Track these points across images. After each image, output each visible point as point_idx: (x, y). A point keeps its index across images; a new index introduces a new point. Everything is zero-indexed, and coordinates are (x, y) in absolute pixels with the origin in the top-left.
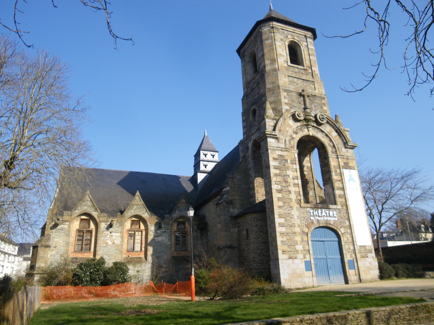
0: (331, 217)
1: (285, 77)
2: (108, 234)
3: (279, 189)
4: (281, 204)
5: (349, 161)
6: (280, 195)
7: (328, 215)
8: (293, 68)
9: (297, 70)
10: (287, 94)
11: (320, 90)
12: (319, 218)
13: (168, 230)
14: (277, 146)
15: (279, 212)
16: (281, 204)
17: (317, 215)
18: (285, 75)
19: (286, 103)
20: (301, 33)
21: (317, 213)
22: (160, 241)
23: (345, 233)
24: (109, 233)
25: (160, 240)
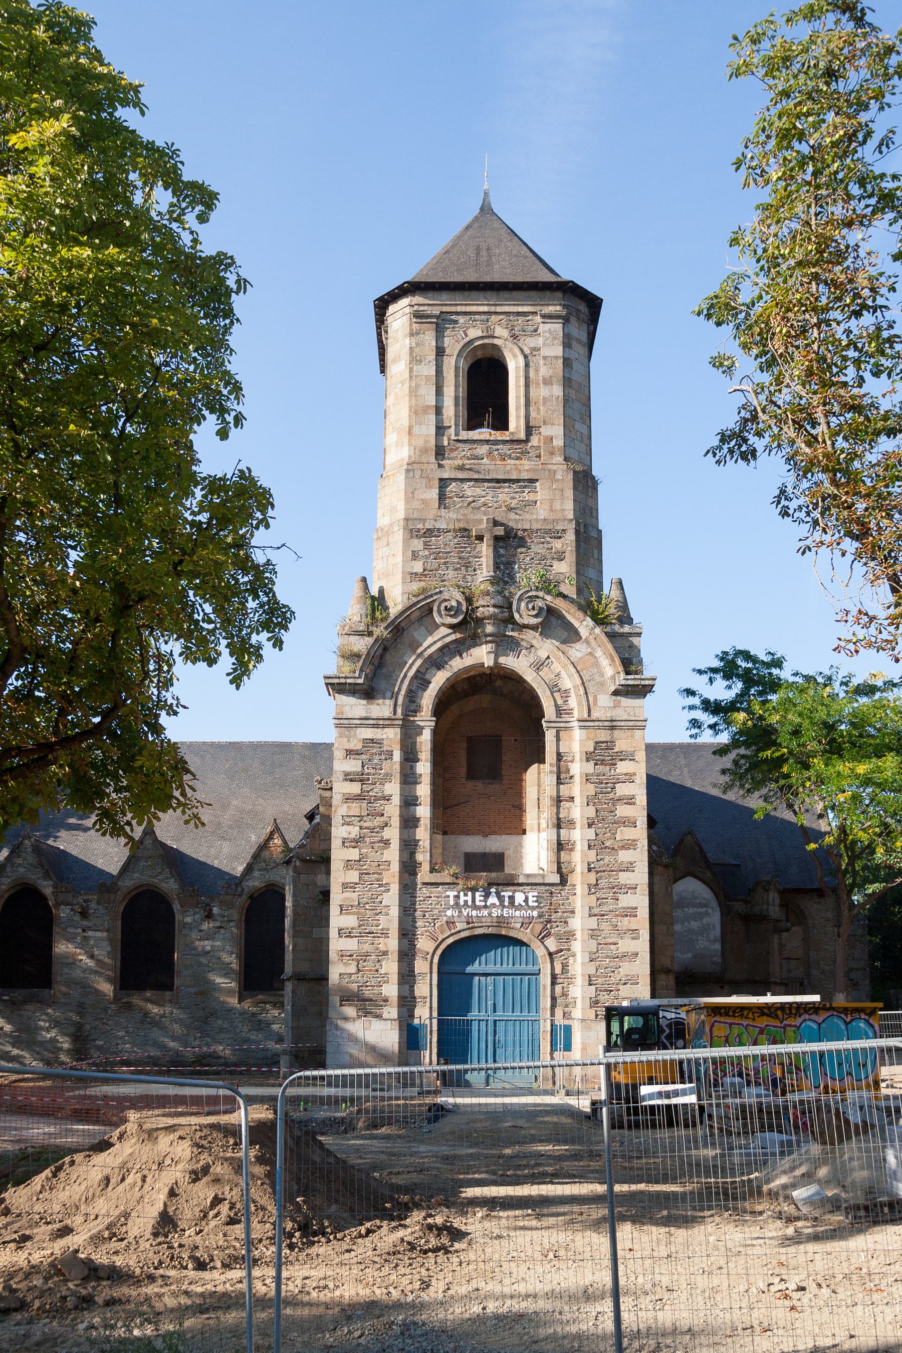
1: (429, 487)
2: (77, 934)
3: (352, 836)
4: (353, 876)
5: (616, 732)
6: (354, 854)
7: (506, 904)
10: (425, 544)
11: (557, 506)
12: (474, 913)
14: (364, 714)
15: (346, 899)
16: (353, 876)
17: (470, 903)
18: (430, 480)
19: (416, 574)
21: (469, 898)
22: (209, 952)
23: (561, 951)
24: (80, 930)
25: (208, 948)
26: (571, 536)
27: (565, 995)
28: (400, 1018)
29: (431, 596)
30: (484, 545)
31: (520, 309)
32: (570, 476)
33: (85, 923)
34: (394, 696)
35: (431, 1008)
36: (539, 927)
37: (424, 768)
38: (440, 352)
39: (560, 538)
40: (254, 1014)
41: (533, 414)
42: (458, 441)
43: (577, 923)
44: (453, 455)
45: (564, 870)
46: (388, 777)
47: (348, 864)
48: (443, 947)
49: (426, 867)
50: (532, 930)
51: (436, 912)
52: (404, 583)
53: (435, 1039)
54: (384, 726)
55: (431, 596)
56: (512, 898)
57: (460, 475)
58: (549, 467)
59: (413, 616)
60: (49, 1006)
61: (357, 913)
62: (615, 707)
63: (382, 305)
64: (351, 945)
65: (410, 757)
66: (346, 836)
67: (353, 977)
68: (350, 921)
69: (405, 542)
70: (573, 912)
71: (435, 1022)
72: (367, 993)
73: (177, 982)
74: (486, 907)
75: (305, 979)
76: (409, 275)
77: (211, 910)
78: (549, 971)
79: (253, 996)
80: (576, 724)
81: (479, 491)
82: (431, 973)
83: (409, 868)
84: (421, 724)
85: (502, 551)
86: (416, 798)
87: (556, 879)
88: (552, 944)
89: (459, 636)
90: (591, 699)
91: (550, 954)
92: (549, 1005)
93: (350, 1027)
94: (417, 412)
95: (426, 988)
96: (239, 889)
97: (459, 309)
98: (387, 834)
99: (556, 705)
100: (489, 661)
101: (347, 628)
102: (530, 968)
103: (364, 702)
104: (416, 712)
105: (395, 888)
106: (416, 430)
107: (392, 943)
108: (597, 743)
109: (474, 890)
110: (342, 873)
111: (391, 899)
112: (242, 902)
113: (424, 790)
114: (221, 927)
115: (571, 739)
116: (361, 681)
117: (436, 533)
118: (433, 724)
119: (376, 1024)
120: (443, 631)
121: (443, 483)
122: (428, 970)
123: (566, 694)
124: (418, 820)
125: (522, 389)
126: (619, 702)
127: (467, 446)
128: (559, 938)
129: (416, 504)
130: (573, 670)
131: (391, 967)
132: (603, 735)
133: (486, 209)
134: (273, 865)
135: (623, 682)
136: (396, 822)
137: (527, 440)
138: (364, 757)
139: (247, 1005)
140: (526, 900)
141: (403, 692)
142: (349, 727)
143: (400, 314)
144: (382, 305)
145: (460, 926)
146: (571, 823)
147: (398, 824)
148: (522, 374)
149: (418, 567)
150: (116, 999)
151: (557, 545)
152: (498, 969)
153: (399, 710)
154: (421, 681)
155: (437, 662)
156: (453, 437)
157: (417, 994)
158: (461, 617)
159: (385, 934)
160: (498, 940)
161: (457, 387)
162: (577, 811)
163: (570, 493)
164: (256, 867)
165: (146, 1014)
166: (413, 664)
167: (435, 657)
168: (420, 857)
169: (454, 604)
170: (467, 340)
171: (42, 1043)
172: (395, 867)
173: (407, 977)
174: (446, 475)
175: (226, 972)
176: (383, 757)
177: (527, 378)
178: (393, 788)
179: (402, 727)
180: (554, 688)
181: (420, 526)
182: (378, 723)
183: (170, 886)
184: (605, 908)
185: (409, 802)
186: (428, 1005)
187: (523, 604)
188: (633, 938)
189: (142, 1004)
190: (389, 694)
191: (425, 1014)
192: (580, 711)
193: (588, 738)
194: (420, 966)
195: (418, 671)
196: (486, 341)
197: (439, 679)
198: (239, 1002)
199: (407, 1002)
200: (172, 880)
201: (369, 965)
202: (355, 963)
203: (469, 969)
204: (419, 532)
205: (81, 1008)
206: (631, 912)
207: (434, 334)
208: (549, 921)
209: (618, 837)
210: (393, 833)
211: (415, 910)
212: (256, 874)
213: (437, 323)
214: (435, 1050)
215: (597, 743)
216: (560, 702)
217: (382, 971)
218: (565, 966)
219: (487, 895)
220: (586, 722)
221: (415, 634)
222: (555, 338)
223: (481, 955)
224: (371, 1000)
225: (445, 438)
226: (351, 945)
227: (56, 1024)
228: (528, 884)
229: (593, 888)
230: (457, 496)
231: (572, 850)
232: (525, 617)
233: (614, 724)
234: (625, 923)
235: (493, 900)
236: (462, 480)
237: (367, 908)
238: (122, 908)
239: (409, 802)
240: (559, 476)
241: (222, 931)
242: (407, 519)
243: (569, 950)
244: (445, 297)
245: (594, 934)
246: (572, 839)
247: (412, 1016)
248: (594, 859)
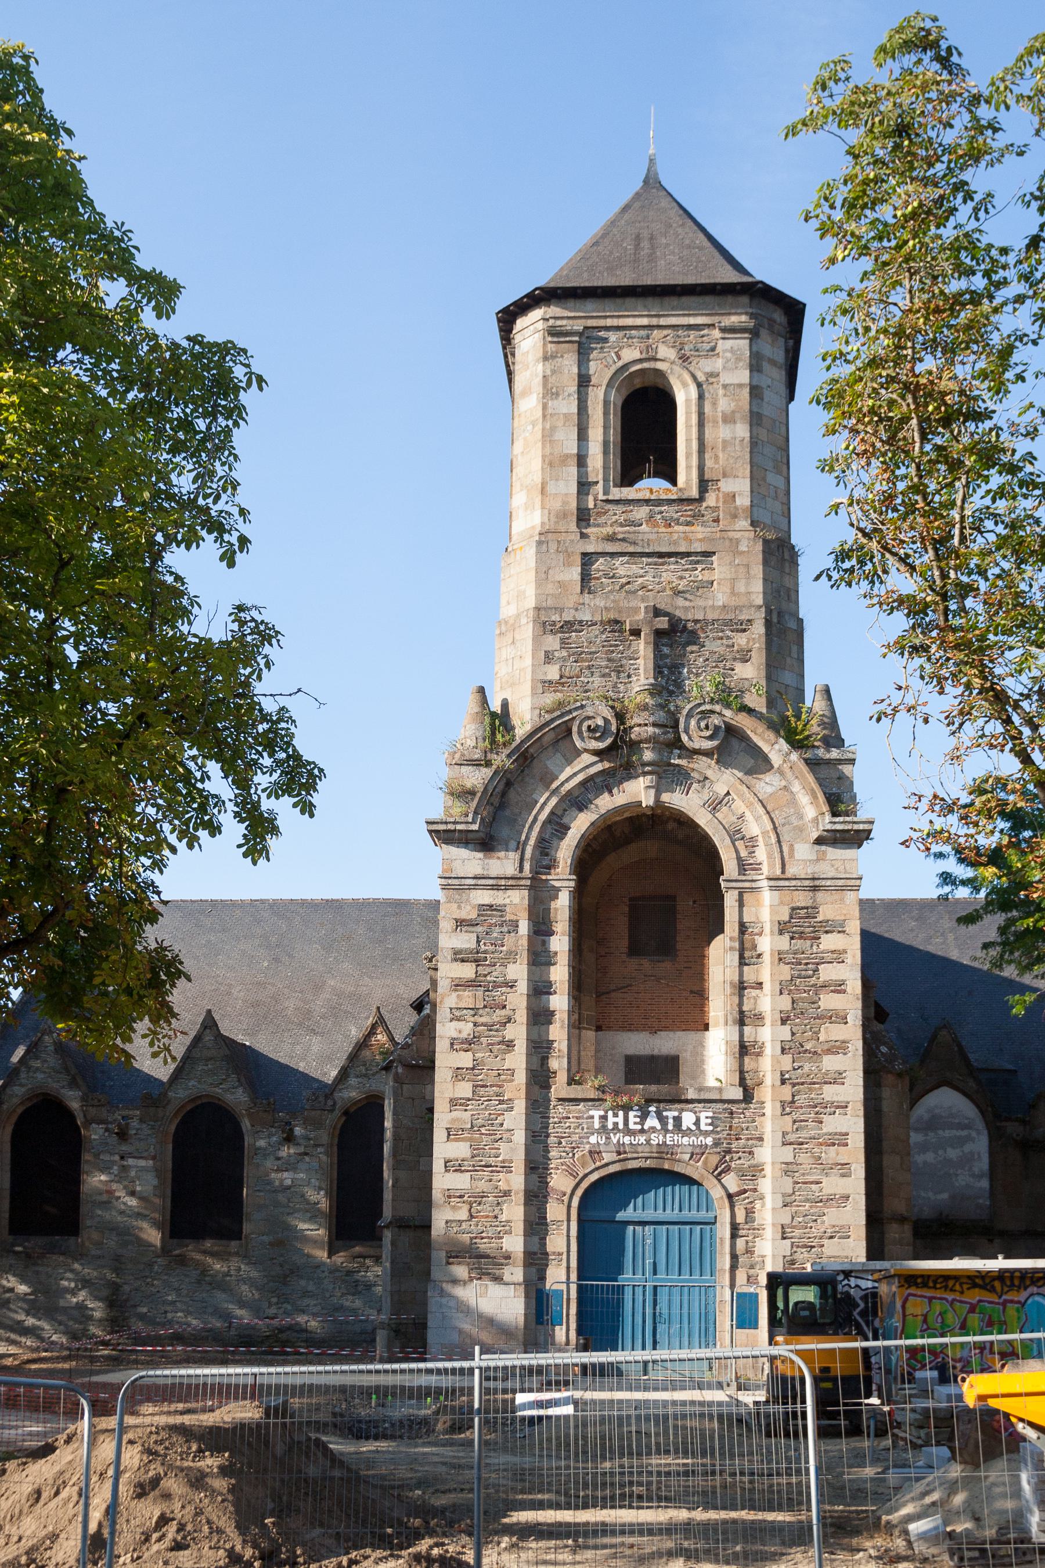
0: (688, 1132)
1: (568, 564)
2: (114, 1162)
3: (464, 1035)
4: (464, 1089)
5: (820, 895)
6: (465, 1060)
7: (670, 1127)
10: (564, 642)
11: (741, 587)
12: (627, 1140)
13: (317, 1146)
14: (479, 871)
15: (454, 1120)
16: (464, 1089)
17: (621, 1126)
18: (569, 555)
21: (620, 1120)
22: (289, 1188)
23: (745, 1191)
24: (117, 1158)
25: (289, 1182)
26: (759, 629)
27: (749, 1251)
28: (527, 1283)
29: (570, 712)
30: (642, 641)
31: (692, 321)
32: (759, 547)
33: (124, 1148)
34: (521, 847)
35: (568, 1268)
36: (714, 1160)
37: (560, 943)
38: (584, 381)
39: (744, 631)
40: (349, 1273)
41: (709, 463)
42: (607, 501)
43: (767, 1154)
44: (602, 520)
45: (749, 1082)
46: (511, 956)
47: (458, 1074)
48: (585, 1185)
49: (562, 1077)
50: (705, 1163)
51: (575, 1137)
52: (534, 694)
53: (573, 1310)
54: (507, 888)
55: (570, 712)
56: (678, 1120)
57: (610, 548)
58: (731, 534)
59: (546, 739)
60: (76, 1259)
61: (470, 1140)
62: (818, 860)
63: (508, 318)
64: (461, 1182)
65: (541, 928)
66: (455, 1035)
67: (464, 1226)
68: (460, 1150)
69: (536, 640)
70: (761, 1139)
71: (574, 1288)
72: (484, 1246)
73: (247, 1228)
74: (642, 1131)
75: (409, 1227)
76: (543, 278)
77: (291, 1130)
78: (728, 1219)
79: (346, 1248)
80: (765, 883)
81: (635, 569)
82: (569, 1220)
83: (539, 1078)
84: (557, 884)
85: (666, 650)
86: (550, 984)
87: (737, 1093)
88: (731, 1182)
89: (607, 765)
90: (785, 849)
91: (730, 1196)
92: (727, 1266)
93: (460, 1292)
94: (552, 463)
95: (562, 1240)
96: (330, 1103)
97: (609, 322)
98: (510, 1032)
99: (739, 858)
100: (647, 800)
101: (457, 756)
102: (703, 1215)
103: (480, 855)
104: (549, 868)
105: (520, 1106)
106: (551, 488)
107: (516, 1180)
108: (793, 909)
109: (627, 1108)
110: (450, 1085)
111: (516, 1120)
112: (333, 1119)
113: (560, 974)
114: (306, 1154)
115: (759, 904)
116: (475, 827)
117: (577, 627)
118: (572, 884)
119: (495, 1290)
120: (587, 759)
121: (587, 559)
122: (564, 1217)
124: (552, 1013)
125: (694, 430)
126: (824, 853)
127: (620, 508)
128: (742, 1174)
129: (550, 589)
130: (761, 810)
131: (515, 1212)
132: (802, 899)
133: (652, 183)
134: (375, 1069)
135: (829, 827)
136: (522, 1017)
137: (701, 499)
138: (479, 929)
139: (339, 1259)
140: (697, 1123)
141: (532, 842)
142: (460, 889)
143: (531, 328)
144: (508, 318)
145: (607, 1157)
146: (759, 1018)
147: (524, 1020)
148: (694, 408)
149: (553, 673)
150: (165, 1250)
152: (660, 1215)
153: (527, 866)
154: (557, 826)
156: (601, 497)
157: (549, 1248)
158: (609, 741)
159: (506, 1167)
160: (659, 1176)
161: (606, 428)
162: (767, 1002)
163: (758, 570)
164: (352, 1072)
165: (204, 1271)
166: (546, 804)
168: (554, 1064)
169: (600, 722)
170: (620, 364)
171: (65, 1310)
172: (521, 1077)
173: (536, 1226)
174: (591, 548)
175: (312, 1213)
176: (505, 929)
177: (701, 414)
178: (519, 971)
179: (531, 888)
180: (735, 835)
181: (555, 617)
182: (499, 884)
183: (237, 1097)
184: (804, 1134)
185: (540, 989)
186: (564, 1263)
187: (693, 722)
188: (843, 1176)
189: (198, 1257)
190: (513, 844)
191: (560, 1277)
192: (771, 866)
193: (782, 903)
194: (554, 1211)
195: (552, 813)
196: (646, 365)
197: (581, 824)
198: (329, 1257)
199: (536, 1260)
200: (240, 1090)
201: (485, 1210)
202: (466, 1207)
203: (621, 1216)
204: (555, 625)
205: (117, 1263)
206: (840, 1140)
207: (575, 357)
208: (729, 1151)
209: (822, 1037)
210: (518, 1032)
211: (548, 1136)
212: (353, 1081)
213: (579, 343)
214: (573, 1326)
215: (793, 909)
216: (743, 854)
217: (503, 1217)
218: (749, 1212)
219: (644, 1117)
220: (780, 881)
221: (550, 764)
222: (738, 359)
223: (636, 1197)
224: (488, 1257)
225: (591, 498)
226: (461, 1182)
227: (85, 1283)
228: (699, 1101)
229: (787, 1106)
230: (606, 576)
231: (759, 1054)
232: (696, 739)
233: (817, 883)
234: (832, 1154)
235: (652, 1122)
236: (613, 555)
237: (483, 1133)
238: (173, 1127)
239: (540, 989)
240: (743, 547)
241: (307, 1159)
242: (538, 609)
243: (755, 1190)
244: (590, 307)
245: (788, 1169)
246: (760, 1039)
247: (542, 1278)
248: (789, 1067)
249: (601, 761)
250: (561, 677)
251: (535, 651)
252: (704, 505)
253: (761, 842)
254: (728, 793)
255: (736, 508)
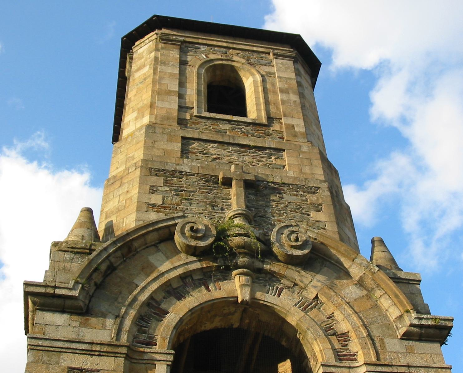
8: (210, 122)
9: (227, 127)
14: (72, 336)
19: (154, 205)
20: (255, 49)
29: (173, 219)
30: (233, 191)
39: (314, 193)
42: (200, 117)
55: (173, 219)
59: (150, 238)
63: (129, 42)
81: (224, 152)
85: (252, 197)
90: (378, 345)
94: (160, 93)
97: (200, 41)
99: (334, 349)
116: (75, 293)
117: (177, 174)
118: (171, 358)
121: (186, 140)
123: (344, 337)
130: (350, 311)
135: (416, 322)
137: (268, 126)
143: (145, 49)
144: (129, 42)
149: (157, 199)
151: (313, 198)
153: (124, 338)
154: (153, 310)
155: (175, 290)
161: (198, 84)
166: (146, 288)
167: (175, 285)
179: (127, 357)
195: (151, 297)
196: (224, 62)
197: (177, 310)
213: (180, 45)
249: (200, 261)
250: (163, 203)
251: (141, 184)
252: (272, 129)
253: (352, 335)
254: (317, 297)
255: (295, 132)
